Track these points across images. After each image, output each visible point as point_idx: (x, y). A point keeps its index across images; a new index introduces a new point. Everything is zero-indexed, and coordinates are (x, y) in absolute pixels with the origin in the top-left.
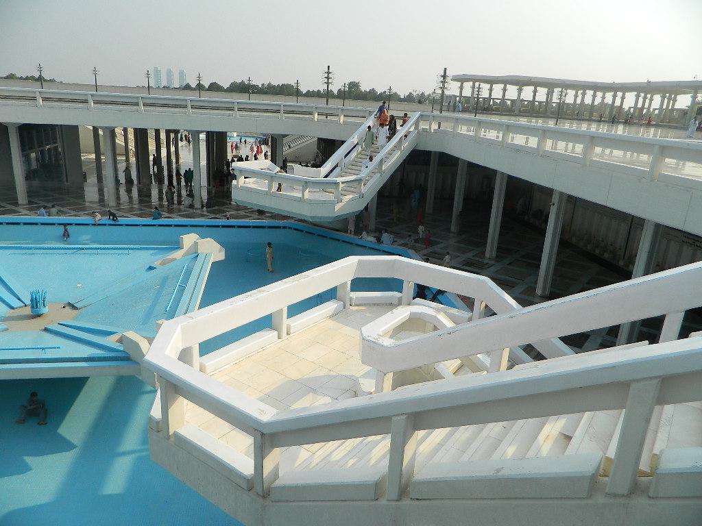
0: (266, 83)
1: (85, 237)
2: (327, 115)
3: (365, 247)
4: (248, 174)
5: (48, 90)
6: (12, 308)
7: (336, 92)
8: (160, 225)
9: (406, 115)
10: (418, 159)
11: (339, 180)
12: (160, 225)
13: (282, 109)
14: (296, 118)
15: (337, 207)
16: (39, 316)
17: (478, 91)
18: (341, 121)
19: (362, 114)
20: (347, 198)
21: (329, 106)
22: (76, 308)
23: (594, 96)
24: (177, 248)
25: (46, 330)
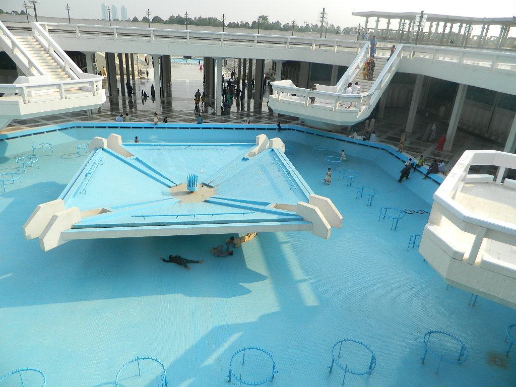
1: (153, 137)
2: (320, 46)
3: (344, 141)
4: (282, 89)
5: (329, 39)
6: (170, 187)
7: (250, 24)
9: (394, 46)
10: (401, 80)
11: (362, 95)
15: (359, 115)
16: (192, 192)
17: (403, 26)
20: (363, 108)
23: (445, 26)
24: (254, 145)
25: (206, 201)
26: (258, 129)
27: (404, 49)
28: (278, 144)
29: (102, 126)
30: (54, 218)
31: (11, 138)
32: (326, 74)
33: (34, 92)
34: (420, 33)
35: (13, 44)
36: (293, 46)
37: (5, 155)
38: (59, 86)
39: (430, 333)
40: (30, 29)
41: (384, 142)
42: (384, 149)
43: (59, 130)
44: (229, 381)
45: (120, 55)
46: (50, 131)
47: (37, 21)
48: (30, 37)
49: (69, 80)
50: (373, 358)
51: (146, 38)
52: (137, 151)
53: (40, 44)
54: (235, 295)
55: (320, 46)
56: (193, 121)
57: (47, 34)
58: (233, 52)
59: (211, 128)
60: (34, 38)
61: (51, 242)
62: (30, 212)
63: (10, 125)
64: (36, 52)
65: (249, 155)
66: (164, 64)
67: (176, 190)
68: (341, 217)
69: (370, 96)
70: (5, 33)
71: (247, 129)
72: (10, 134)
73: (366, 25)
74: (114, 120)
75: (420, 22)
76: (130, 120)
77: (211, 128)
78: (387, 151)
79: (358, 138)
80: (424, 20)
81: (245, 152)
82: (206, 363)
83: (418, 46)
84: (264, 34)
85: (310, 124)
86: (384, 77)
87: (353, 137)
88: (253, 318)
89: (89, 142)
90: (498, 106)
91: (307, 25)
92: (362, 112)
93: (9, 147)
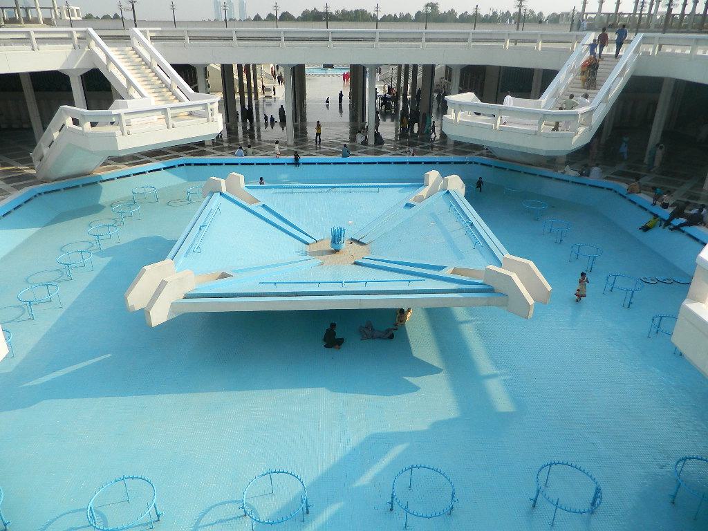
0: (340, 10)
1: (284, 176)
2: (516, 42)
4: (461, 106)
6: (308, 244)
8: (349, 163)
12: (349, 163)
13: (378, 36)
14: (482, 47)
15: (574, 140)
16: (337, 251)
18: (540, 48)
19: (533, 38)
20: (581, 130)
21: (477, 31)
22: (364, 244)
24: (421, 186)
25: (356, 263)
26: (426, 163)
27: (645, 41)
28: (456, 184)
30: (163, 284)
31: (104, 181)
32: (525, 82)
33: (135, 120)
35: (108, 57)
37: (100, 203)
38: (164, 110)
39: (685, 459)
40: (127, 38)
41: (613, 179)
42: (611, 189)
43: (164, 169)
44: (391, 510)
45: (239, 66)
46: (155, 170)
47: (136, 26)
48: (127, 49)
49: (176, 103)
50: (598, 490)
51: (275, 42)
52: (264, 196)
53: (140, 57)
54: (397, 391)
55: (516, 42)
56: (336, 153)
57: (148, 42)
58: (388, 55)
59: (360, 163)
60: (133, 49)
61: (159, 316)
62: (131, 277)
63: (105, 164)
64: (136, 67)
65: (415, 200)
66: (297, 76)
67: (315, 248)
68: (549, 288)
69: (591, 112)
70: (98, 45)
71: (410, 163)
72: (106, 175)
73: (584, 7)
74: (233, 154)
76: (254, 154)
77: (360, 163)
78: (616, 192)
79: (571, 173)
81: (410, 195)
82: (358, 484)
83: (666, 35)
84: (434, 28)
85: (499, 154)
86: (613, 84)
87: (564, 173)
88: (421, 425)
89: (203, 184)
91: (495, 13)
92: (580, 136)
93: (104, 192)
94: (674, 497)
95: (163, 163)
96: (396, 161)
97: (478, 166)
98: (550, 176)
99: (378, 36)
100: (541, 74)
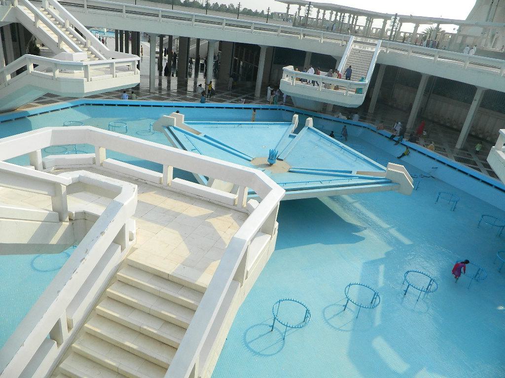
6: (250, 161)
16: (271, 165)
17: (343, 19)
22: (282, 160)
23: (336, 15)
24: (291, 124)
25: (290, 171)
29: (97, 103)
31: (32, 115)
34: (341, 23)
35: (37, 16)
36: (283, 34)
43: (72, 107)
51: (154, 18)
52: (204, 130)
55: (304, 35)
72: (31, 111)
73: (288, 12)
75: (394, 22)
78: (368, 128)
79: (343, 118)
80: (397, 21)
87: (338, 117)
90: (433, 93)
94: (500, 269)
95: (72, 103)
96: (207, 106)
97: (261, 111)
98: (330, 118)
99: (194, 18)
100: (311, 55)
